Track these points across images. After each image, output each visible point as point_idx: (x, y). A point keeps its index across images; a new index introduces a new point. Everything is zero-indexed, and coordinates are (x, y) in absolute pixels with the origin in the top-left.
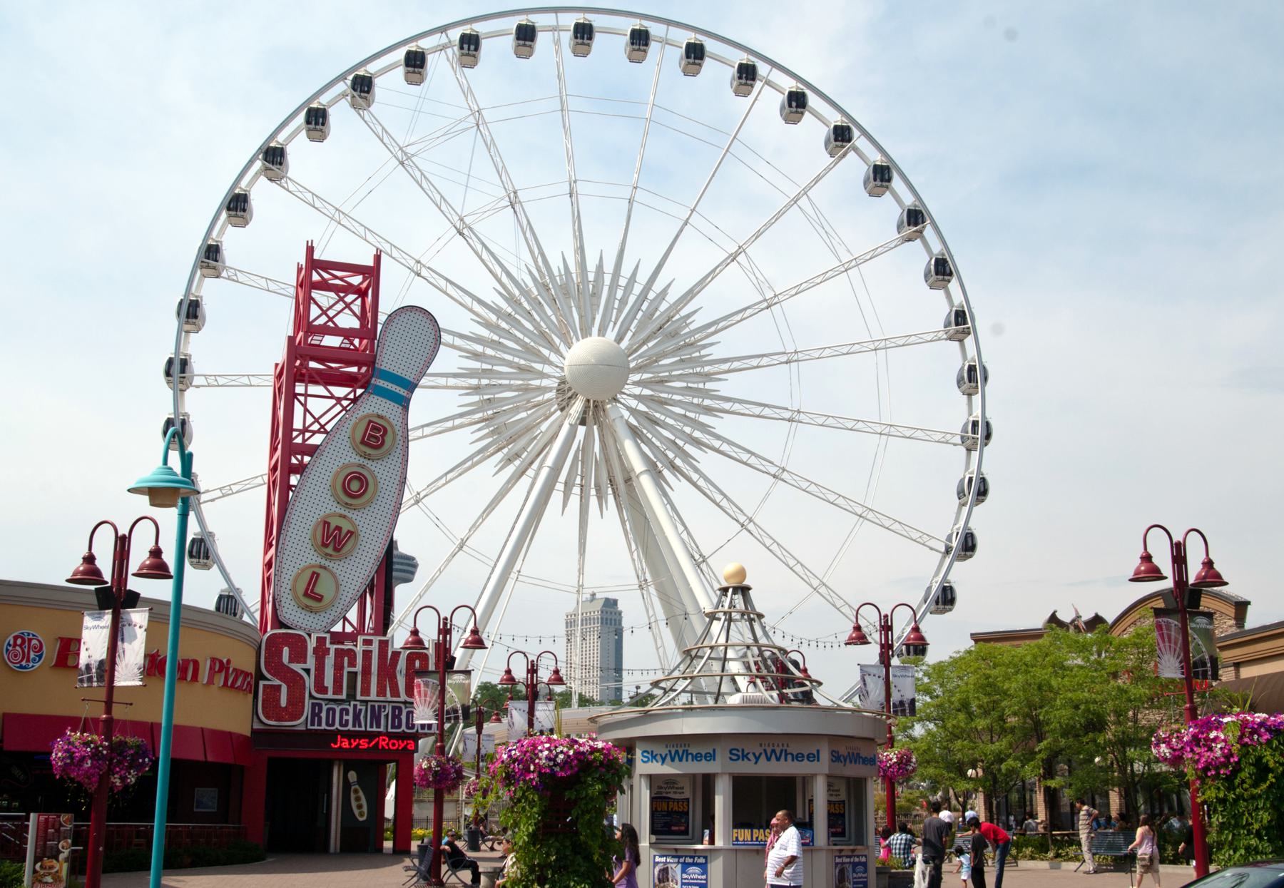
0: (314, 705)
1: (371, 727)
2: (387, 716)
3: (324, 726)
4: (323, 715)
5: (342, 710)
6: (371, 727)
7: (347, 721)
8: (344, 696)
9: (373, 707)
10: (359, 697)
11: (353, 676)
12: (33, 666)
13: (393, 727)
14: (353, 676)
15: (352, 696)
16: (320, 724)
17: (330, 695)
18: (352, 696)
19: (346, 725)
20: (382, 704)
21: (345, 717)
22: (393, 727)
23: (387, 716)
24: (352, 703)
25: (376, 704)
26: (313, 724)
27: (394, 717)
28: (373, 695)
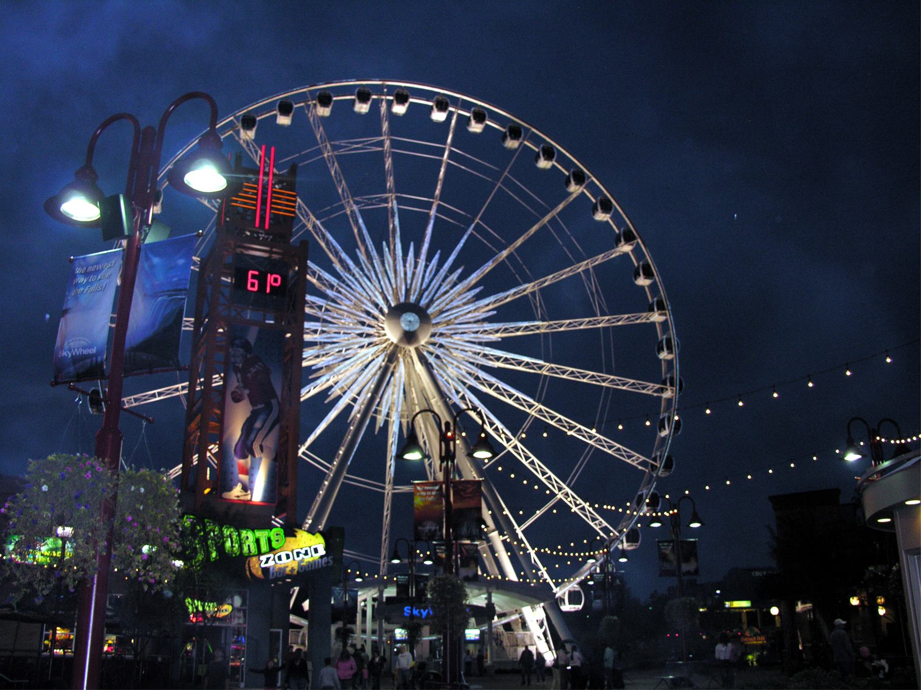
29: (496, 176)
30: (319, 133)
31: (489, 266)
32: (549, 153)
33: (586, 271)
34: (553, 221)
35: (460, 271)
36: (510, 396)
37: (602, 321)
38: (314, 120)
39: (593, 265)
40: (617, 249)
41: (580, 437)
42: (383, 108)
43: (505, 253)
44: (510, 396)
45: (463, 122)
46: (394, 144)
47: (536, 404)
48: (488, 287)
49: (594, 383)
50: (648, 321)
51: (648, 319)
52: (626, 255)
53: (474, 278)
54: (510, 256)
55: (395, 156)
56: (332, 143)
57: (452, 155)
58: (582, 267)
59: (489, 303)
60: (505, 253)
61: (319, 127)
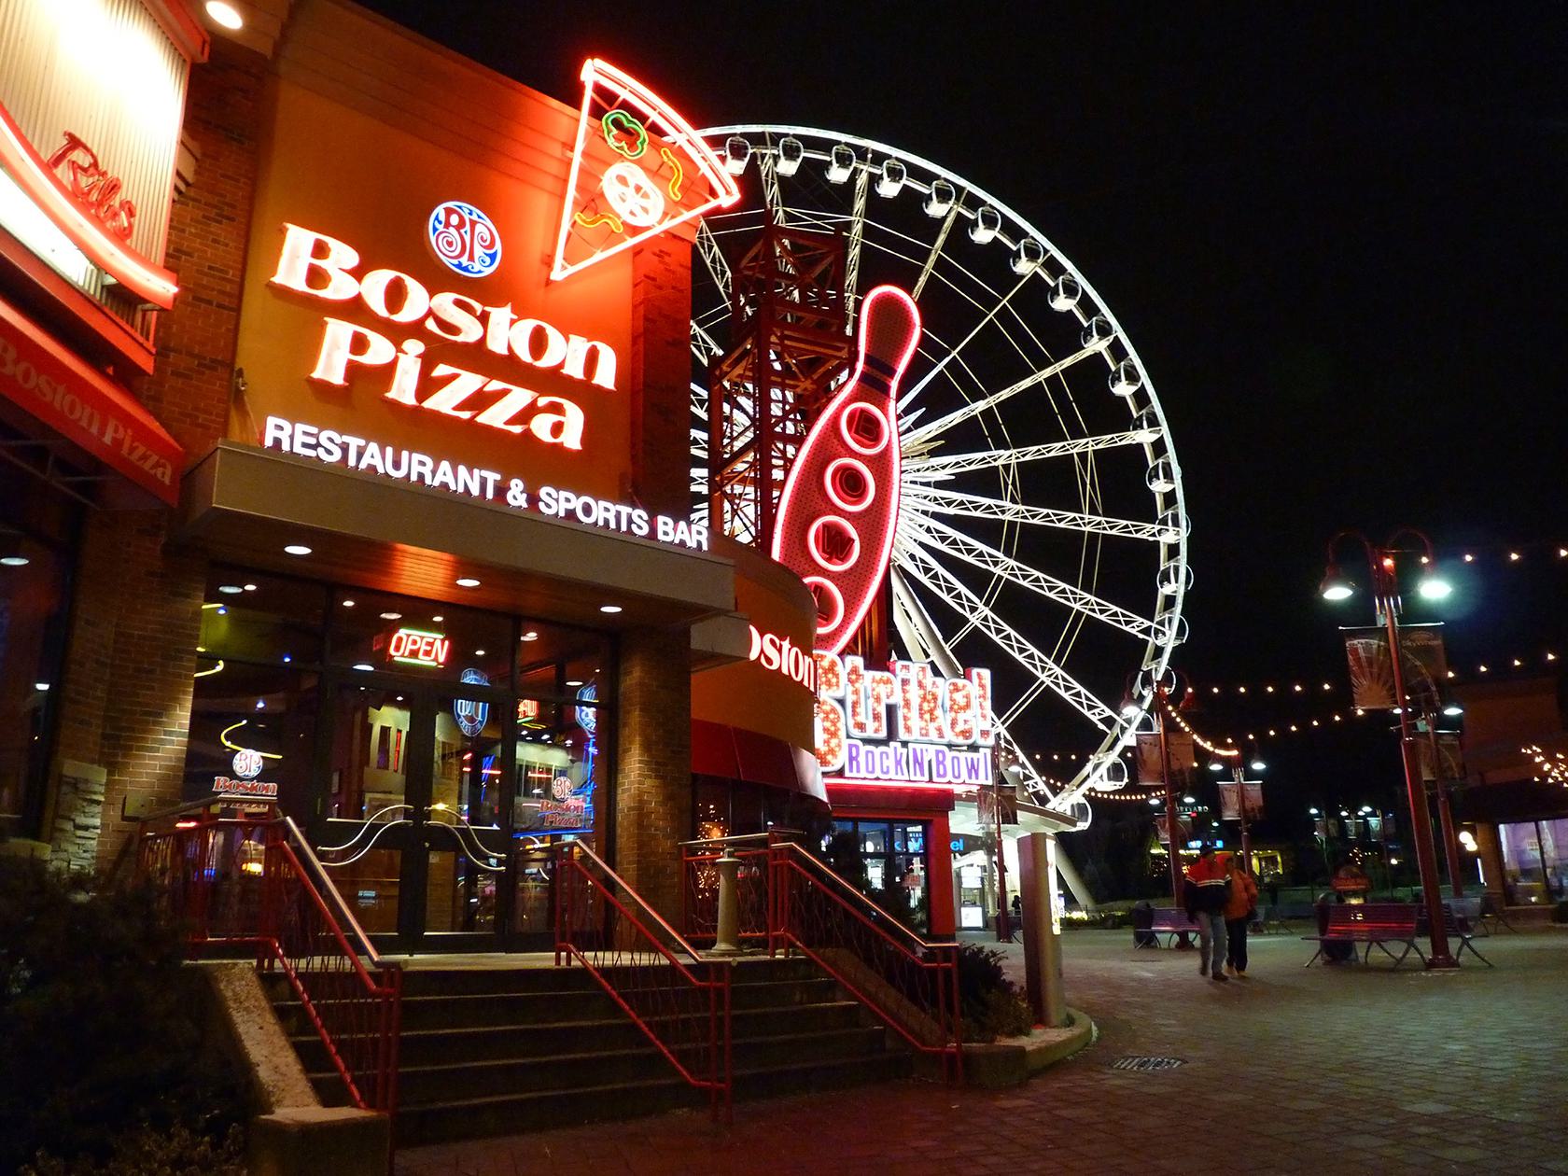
0: (850, 746)
1: (915, 774)
2: (930, 762)
3: (863, 774)
4: (862, 759)
5: (882, 754)
6: (915, 774)
7: (888, 767)
8: (883, 734)
9: (915, 750)
10: (902, 735)
11: (891, 710)
12: (480, 272)
13: (939, 775)
14: (891, 710)
15: (892, 734)
16: (858, 771)
17: (870, 733)
18: (892, 734)
19: (887, 772)
20: (924, 746)
21: (886, 763)
22: (939, 775)
23: (930, 762)
24: (892, 744)
25: (918, 747)
26: (851, 770)
27: (939, 763)
28: (916, 735)
29: (991, 303)
30: (772, 193)
31: (956, 417)
32: (1071, 290)
33: (1083, 456)
34: (1053, 380)
35: (919, 413)
36: (950, 590)
37: (1089, 523)
38: (767, 175)
39: (1096, 448)
40: (1132, 433)
41: (1030, 667)
42: (862, 180)
43: (981, 406)
44: (950, 590)
45: (963, 225)
46: (867, 232)
47: (981, 606)
48: (953, 442)
49: (1062, 601)
50: (1151, 539)
51: (1153, 535)
52: (1140, 446)
53: (935, 427)
54: (987, 413)
55: (864, 248)
56: (788, 209)
57: (940, 264)
58: (1076, 447)
59: (948, 467)
60: (981, 406)
61: (773, 184)
